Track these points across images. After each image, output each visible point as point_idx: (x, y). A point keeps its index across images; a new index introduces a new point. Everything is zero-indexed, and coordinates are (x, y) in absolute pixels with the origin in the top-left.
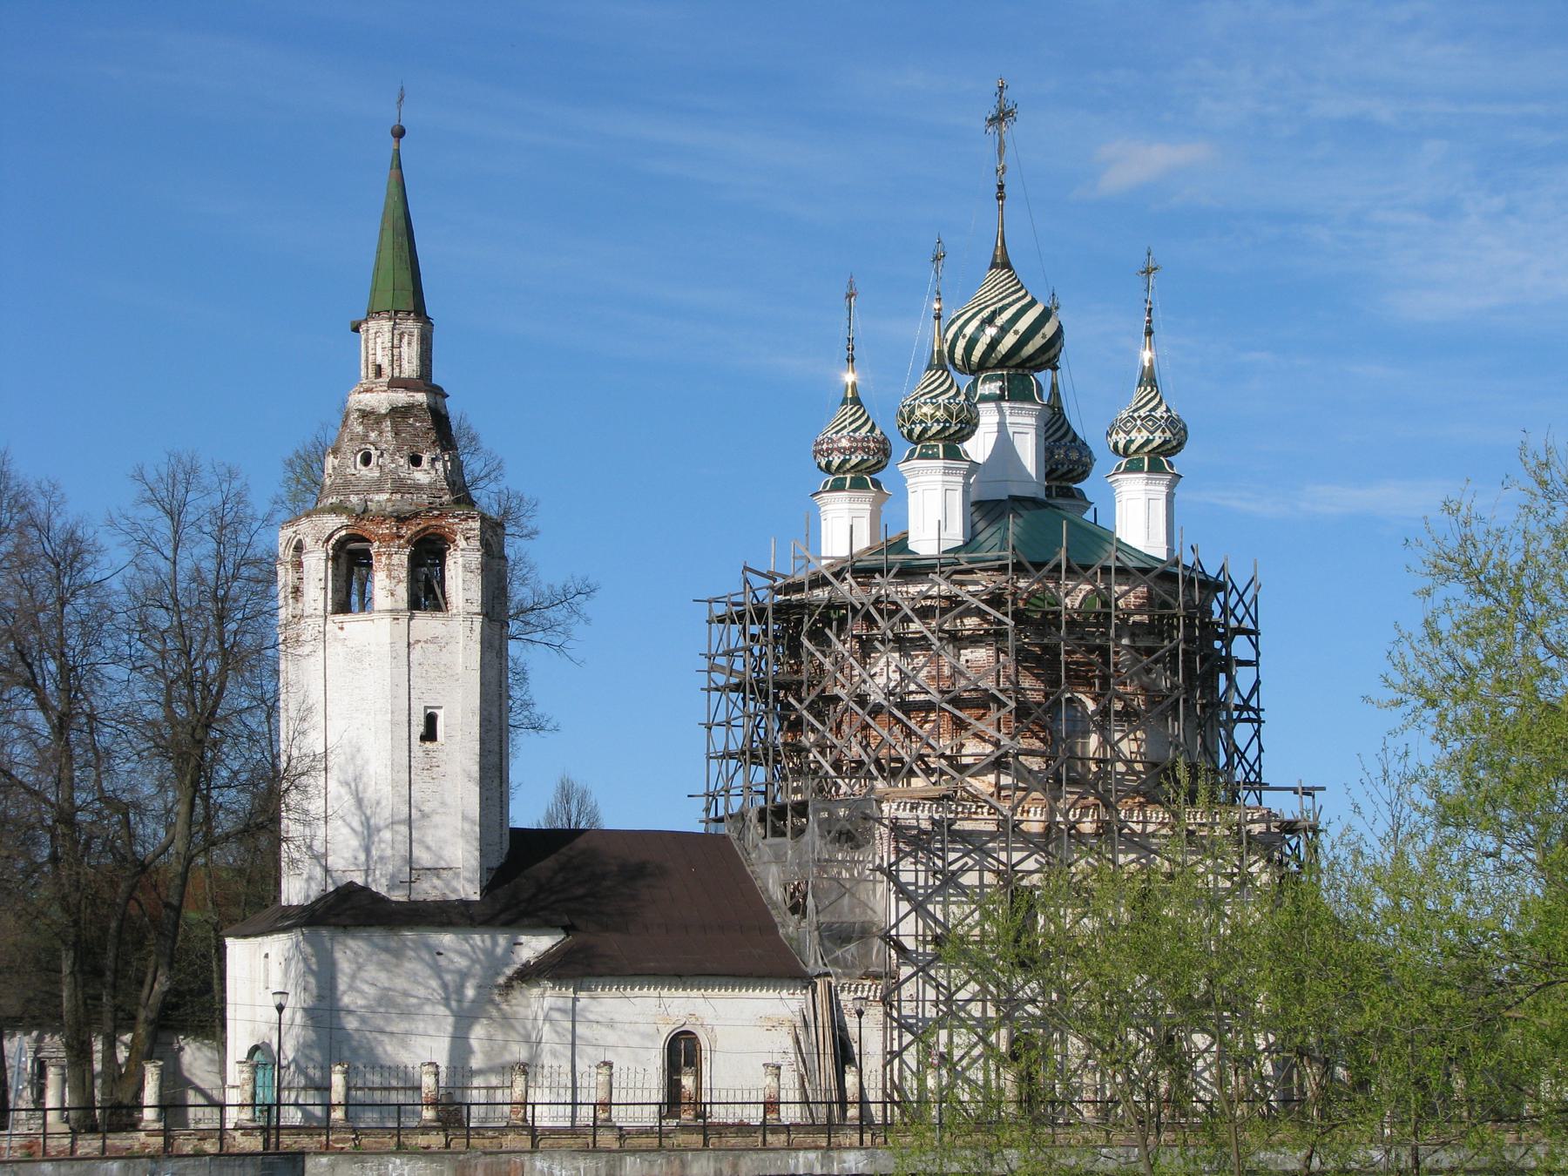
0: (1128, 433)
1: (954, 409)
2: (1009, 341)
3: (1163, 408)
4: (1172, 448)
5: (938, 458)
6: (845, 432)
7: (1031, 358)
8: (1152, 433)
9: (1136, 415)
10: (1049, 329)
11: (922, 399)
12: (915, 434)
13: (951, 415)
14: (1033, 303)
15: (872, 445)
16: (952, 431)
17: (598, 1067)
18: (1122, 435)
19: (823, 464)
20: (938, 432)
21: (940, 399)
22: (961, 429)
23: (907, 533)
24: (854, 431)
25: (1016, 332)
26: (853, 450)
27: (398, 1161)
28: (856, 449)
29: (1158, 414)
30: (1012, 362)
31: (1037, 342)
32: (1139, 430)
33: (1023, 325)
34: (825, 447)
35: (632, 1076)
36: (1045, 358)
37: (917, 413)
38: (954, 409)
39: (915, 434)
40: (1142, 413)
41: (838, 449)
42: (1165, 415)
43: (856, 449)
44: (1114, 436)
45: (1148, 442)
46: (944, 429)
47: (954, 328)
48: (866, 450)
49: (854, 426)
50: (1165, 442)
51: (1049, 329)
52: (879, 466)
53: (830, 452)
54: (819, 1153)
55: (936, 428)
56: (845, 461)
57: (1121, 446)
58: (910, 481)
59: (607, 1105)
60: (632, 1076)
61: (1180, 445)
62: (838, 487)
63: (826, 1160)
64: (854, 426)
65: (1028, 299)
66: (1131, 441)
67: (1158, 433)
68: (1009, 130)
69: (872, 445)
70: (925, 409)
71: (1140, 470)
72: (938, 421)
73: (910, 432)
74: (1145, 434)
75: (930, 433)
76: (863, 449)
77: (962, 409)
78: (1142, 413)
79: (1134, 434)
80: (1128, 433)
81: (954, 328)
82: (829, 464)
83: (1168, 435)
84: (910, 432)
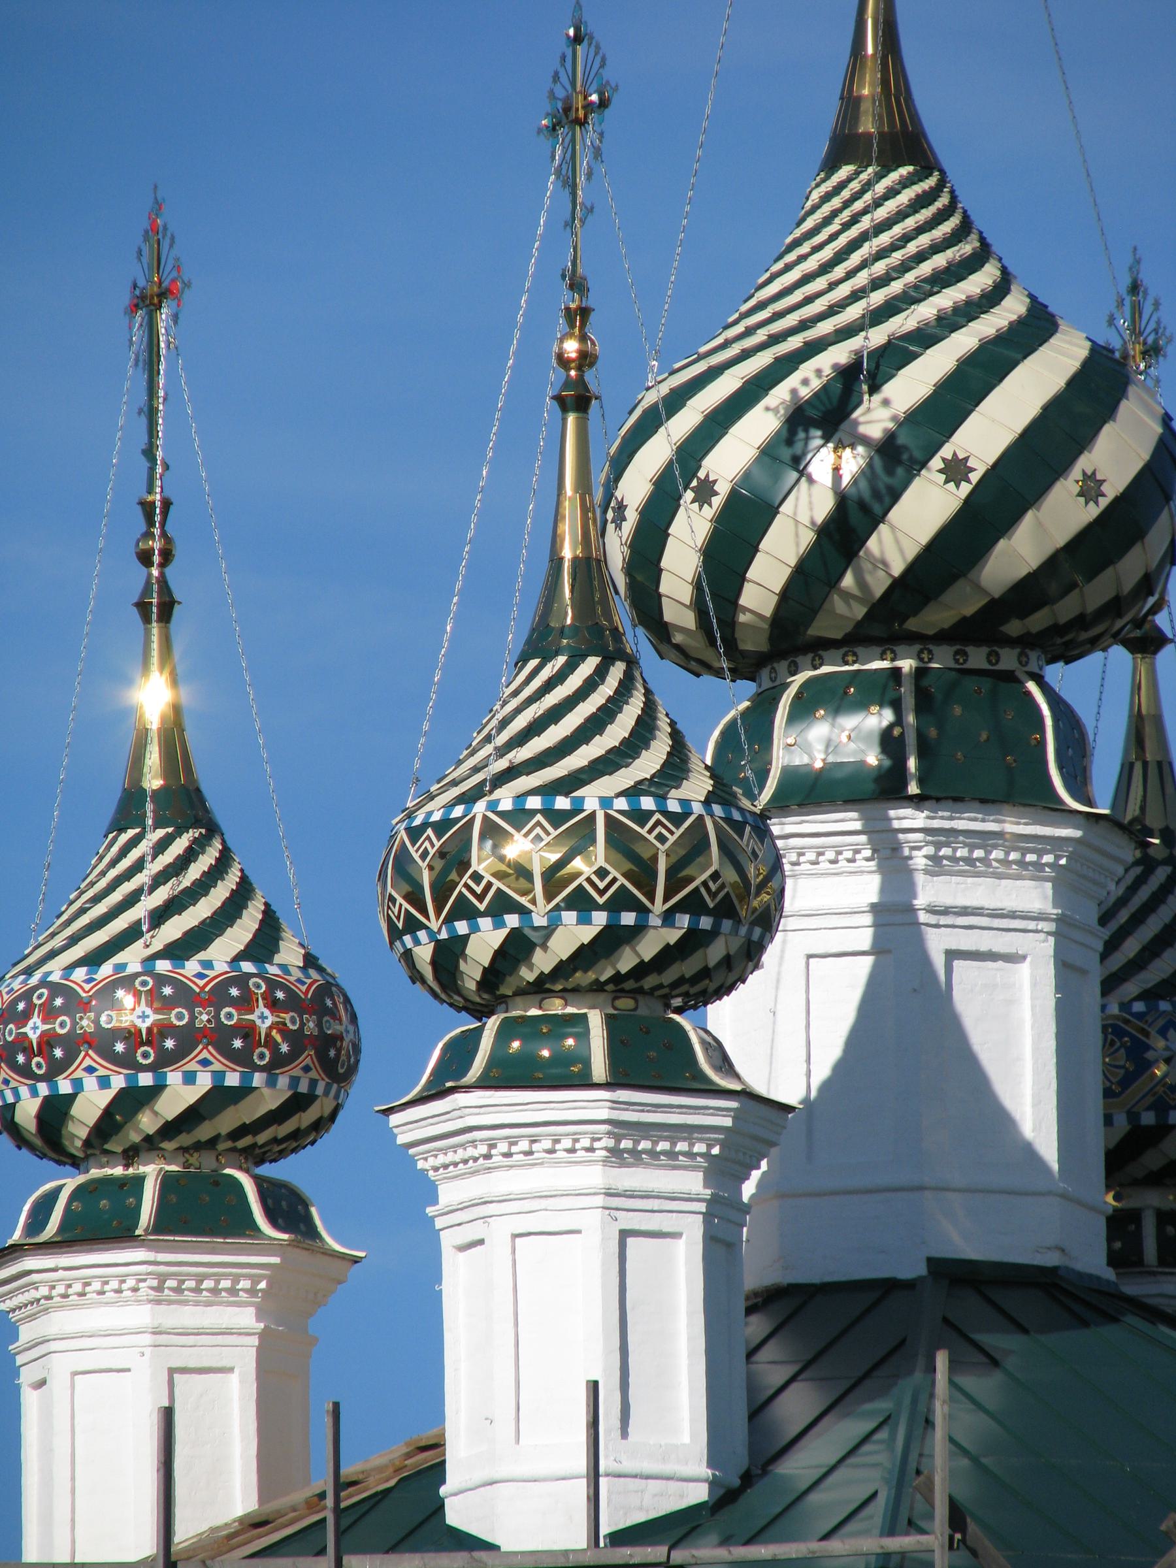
5: (584, 1082)
6: (132, 957)
11: (505, 798)
12: (472, 971)
13: (643, 874)
15: (263, 1019)
16: (648, 947)
19: (28, 1110)
20: (584, 956)
21: (591, 796)
22: (693, 941)
23: (437, 1445)
24: (178, 951)
25: (956, 470)
28: (189, 1039)
34: (34, 1028)
37: (482, 861)
39: (472, 971)
41: (101, 1042)
43: (189, 1039)
49: (174, 929)
58: (449, 1193)
64: (174, 929)
65: (1013, 307)
69: (263, 1019)
70: (518, 847)
72: (581, 902)
75: (543, 962)
76: (219, 1038)
77: (695, 845)
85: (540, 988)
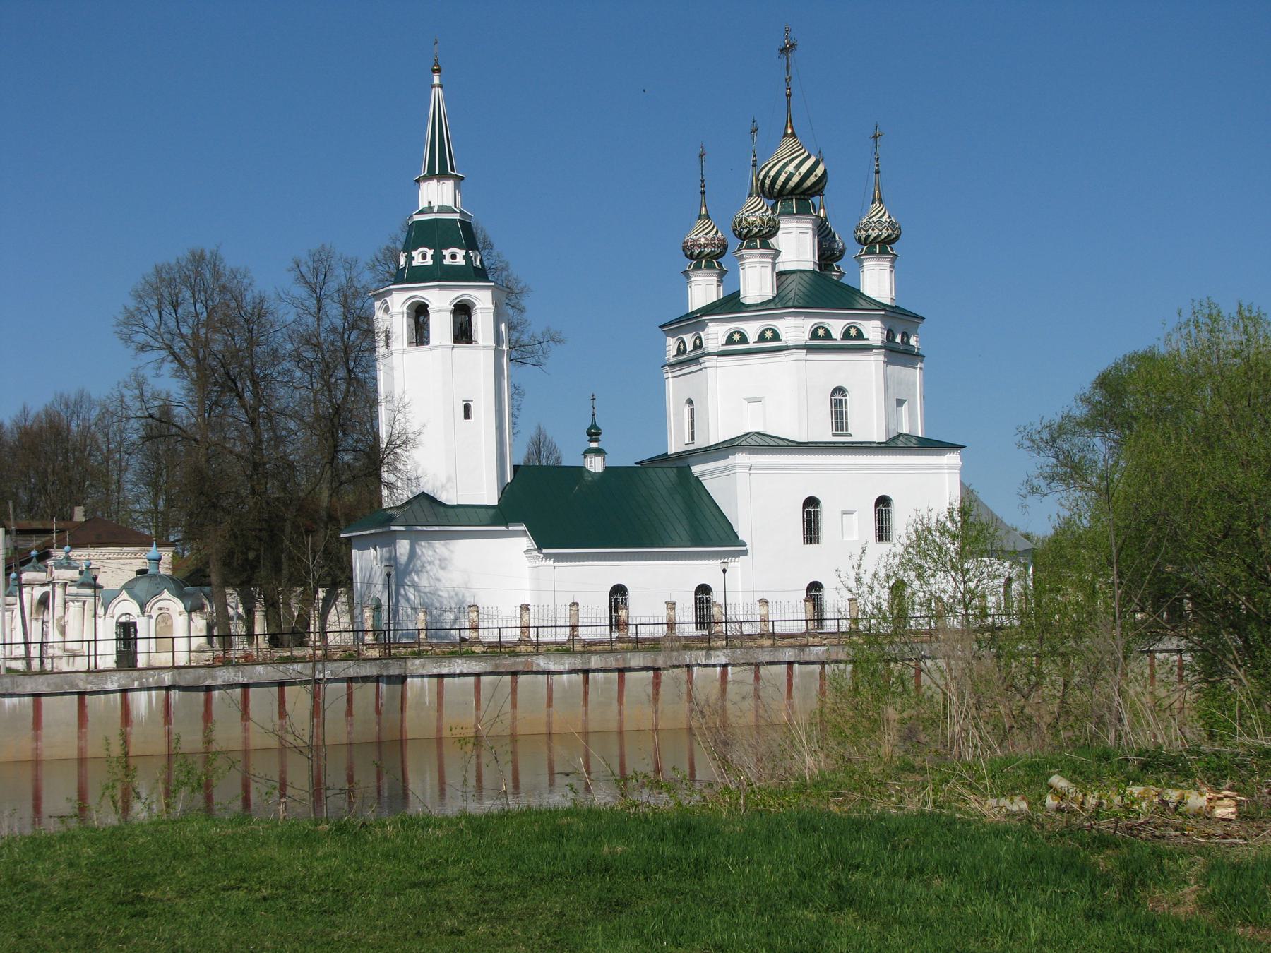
1: (766, 219)
2: (796, 179)
3: (887, 215)
5: (756, 248)
6: (701, 235)
7: (809, 188)
8: (881, 231)
9: (871, 220)
10: (819, 171)
14: (809, 157)
15: (717, 242)
16: (764, 232)
17: (570, 606)
18: (863, 232)
20: (757, 233)
21: (757, 214)
23: (739, 291)
24: (706, 234)
26: (706, 245)
27: (460, 661)
28: (707, 245)
29: (884, 219)
30: (797, 192)
31: (812, 179)
32: (873, 230)
33: (803, 169)
34: (689, 244)
35: (590, 610)
36: (817, 189)
40: (875, 219)
41: (697, 245)
42: (888, 220)
44: (858, 233)
45: (879, 236)
46: (760, 231)
47: (763, 173)
50: (889, 236)
52: (721, 254)
53: (692, 247)
54: (704, 652)
55: (756, 230)
56: (701, 252)
59: (574, 628)
60: (590, 610)
61: (898, 237)
63: (708, 656)
65: (806, 154)
67: (884, 231)
69: (717, 242)
71: (874, 253)
72: (756, 226)
73: (740, 233)
74: (876, 231)
76: (712, 244)
77: (770, 219)
78: (875, 219)
79: (870, 231)
80: (867, 231)
81: (763, 173)
82: (692, 253)
83: (890, 231)
85: (752, 237)
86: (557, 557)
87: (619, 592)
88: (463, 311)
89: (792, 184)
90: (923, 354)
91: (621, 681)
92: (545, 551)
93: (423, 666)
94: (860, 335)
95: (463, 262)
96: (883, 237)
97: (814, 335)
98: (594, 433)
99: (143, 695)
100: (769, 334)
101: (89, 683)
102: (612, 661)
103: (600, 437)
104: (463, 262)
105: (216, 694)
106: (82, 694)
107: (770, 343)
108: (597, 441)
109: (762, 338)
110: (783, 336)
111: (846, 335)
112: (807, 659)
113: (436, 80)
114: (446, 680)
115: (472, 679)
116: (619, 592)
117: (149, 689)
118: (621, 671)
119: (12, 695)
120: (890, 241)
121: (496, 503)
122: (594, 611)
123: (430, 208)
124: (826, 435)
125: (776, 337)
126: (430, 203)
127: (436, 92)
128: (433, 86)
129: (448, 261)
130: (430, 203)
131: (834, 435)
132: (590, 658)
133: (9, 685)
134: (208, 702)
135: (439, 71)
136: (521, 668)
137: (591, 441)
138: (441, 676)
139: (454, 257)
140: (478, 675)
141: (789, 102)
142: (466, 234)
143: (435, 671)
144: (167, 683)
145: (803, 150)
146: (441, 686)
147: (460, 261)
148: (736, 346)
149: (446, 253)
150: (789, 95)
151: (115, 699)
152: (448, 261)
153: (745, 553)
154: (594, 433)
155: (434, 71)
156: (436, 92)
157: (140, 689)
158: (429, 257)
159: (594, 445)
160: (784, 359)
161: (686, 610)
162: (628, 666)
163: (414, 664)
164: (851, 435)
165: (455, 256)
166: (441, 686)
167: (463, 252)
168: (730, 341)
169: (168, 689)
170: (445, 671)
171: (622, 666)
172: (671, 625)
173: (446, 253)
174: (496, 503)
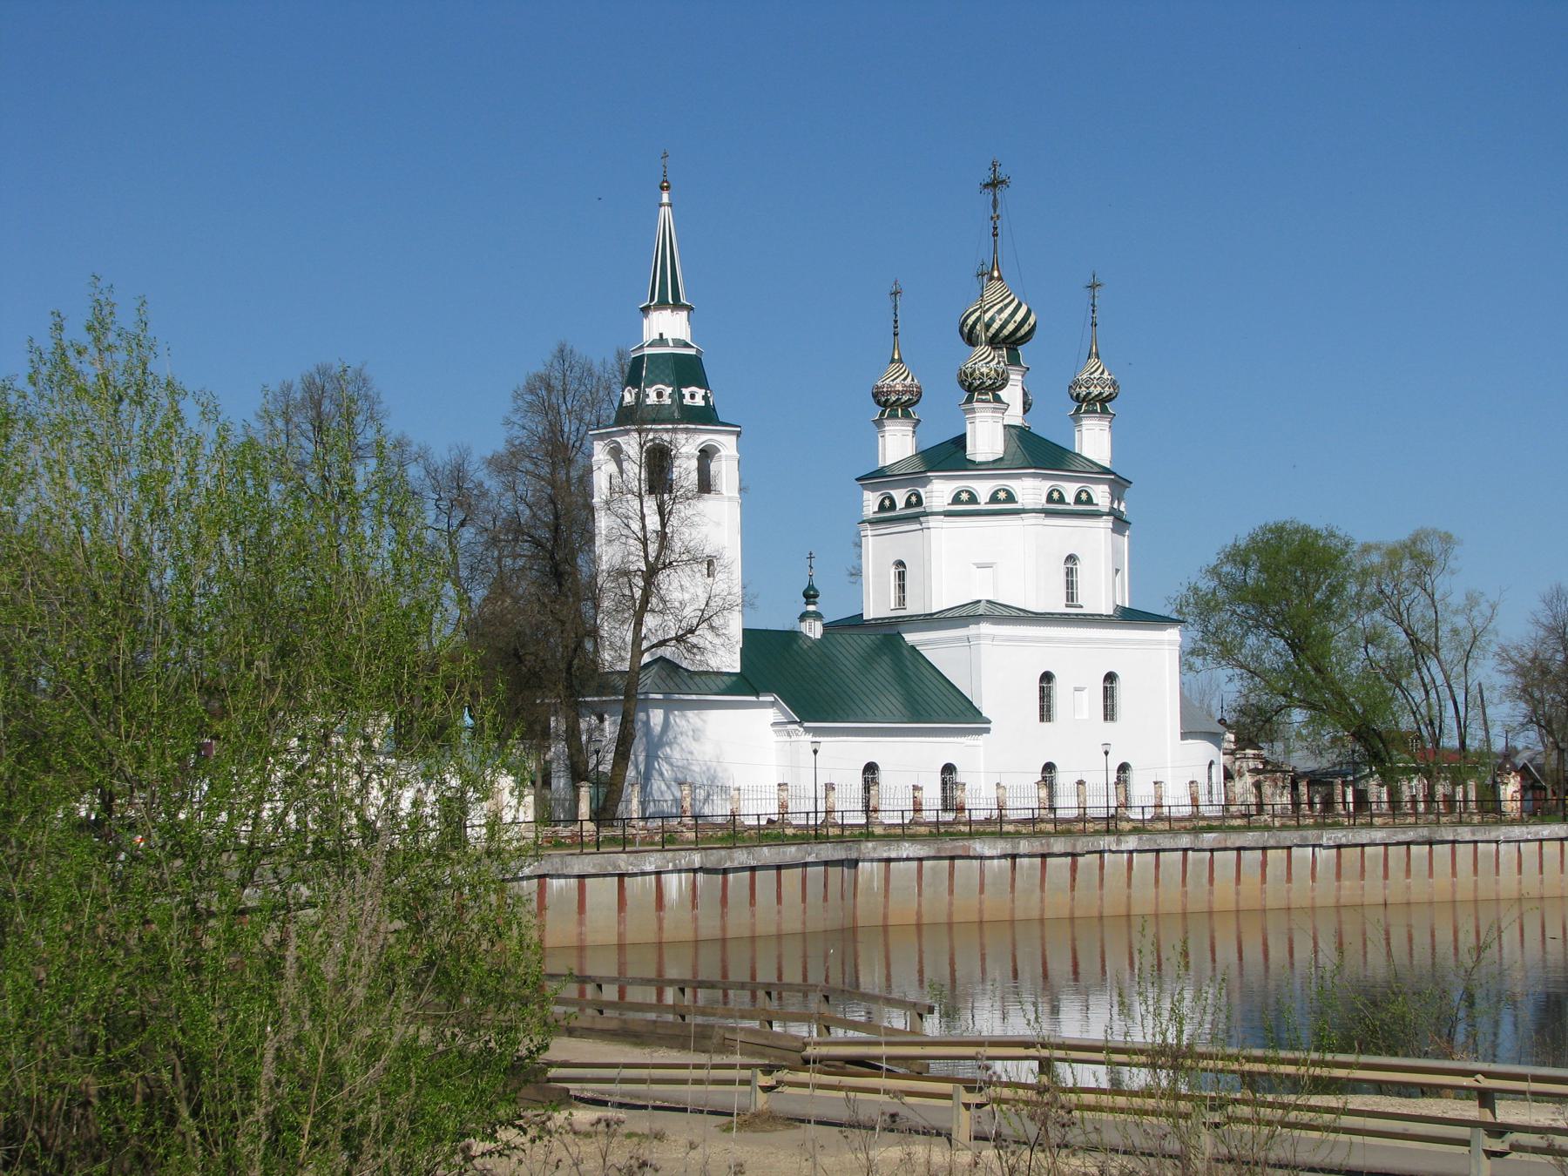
0: (1088, 388)
1: (1000, 371)
2: (1011, 327)
4: (1110, 398)
6: (898, 381)
7: (1007, 337)
8: (1103, 388)
14: (1019, 305)
18: (1083, 389)
21: (991, 364)
27: (907, 845)
28: (906, 391)
30: (1010, 341)
31: (1026, 328)
32: (1095, 387)
38: (1000, 371)
40: (1097, 375)
41: (895, 392)
45: (1101, 394)
46: (994, 383)
47: (973, 318)
48: (911, 392)
50: (1110, 394)
51: (1032, 320)
52: (913, 404)
53: (889, 393)
56: (898, 399)
57: (1082, 396)
62: (893, 416)
63: (1119, 842)
65: (1016, 302)
66: (1090, 393)
67: (1107, 389)
68: (1001, 193)
72: (990, 379)
73: (971, 384)
74: (1099, 389)
76: (910, 391)
79: (1092, 389)
80: (1088, 388)
81: (973, 318)
83: (1112, 390)
84: (971, 384)
85: (983, 389)
86: (816, 732)
87: (871, 769)
88: (706, 454)
89: (1006, 332)
90: (1128, 519)
91: (1044, 865)
92: (806, 724)
93: (875, 849)
94: (1090, 501)
95: (702, 403)
96: (1104, 395)
97: (1050, 499)
98: (810, 595)
99: (675, 876)
100: (1002, 495)
101: (631, 864)
102: (1037, 846)
103: (817, 600)
104: (702, 403)
105: (731, 876)
106: (621, 876)
107: (1004, 505)
108: (814, 603)
109: (994, 499)
110: (1019, 496)
111: (1078, 500)
112: (1200, 846)
113: (665, 198)
114: (892, 864)
115: (915, 864)
116: (871, 769)
117: (680, 871)
118: (1044, 856)
119: (559, 876)
120: (1110, 398)
121: (738, 670)
122: (893, 791)
123: (661, 341)
124: (1059, 606)
125: (1010, 498)
126: (661, 335)
127: (665, 212)
128: (661, 205)
129: (687, 401)
130: (661, 335)
131: (1067, 606)
132: (1019, 843)
133: (559, 866)
134: (725, 882)
135: (668, 188)
136: (960, 852)
137: (807, 604)
138: (888, 860)
139: (692, 396)
140: (920, 860)
141: (995, 241)
142: (686, 370)
143: (885, 855)
144: (697, 865)
145: (1012, 297)
146: (888, 870)
147: (699, 401)
148: (964, 507)
149: (686, 392)
150: (995, 235)
151: (650, 879)
152: (687, 401)
153: (987, 730)
154: (810, 595)
155: (662, 188)
156: (665, 212)
157: (672, 872)
158: (687, 396)
159: (811, 608)
160: (1020, 522)
161: (932, 795)
162: (1051, 851)
163: (867, 847)
164: (1081, 607)
165: (695, 397)
166: (888, 870)
167: (669, 390)
168: (956, 500)
169: (695, 871)
170: (893, 855)
171: (1046, 851)
172: (917, 808)
173: (686, 392)
174: (738, 670)
